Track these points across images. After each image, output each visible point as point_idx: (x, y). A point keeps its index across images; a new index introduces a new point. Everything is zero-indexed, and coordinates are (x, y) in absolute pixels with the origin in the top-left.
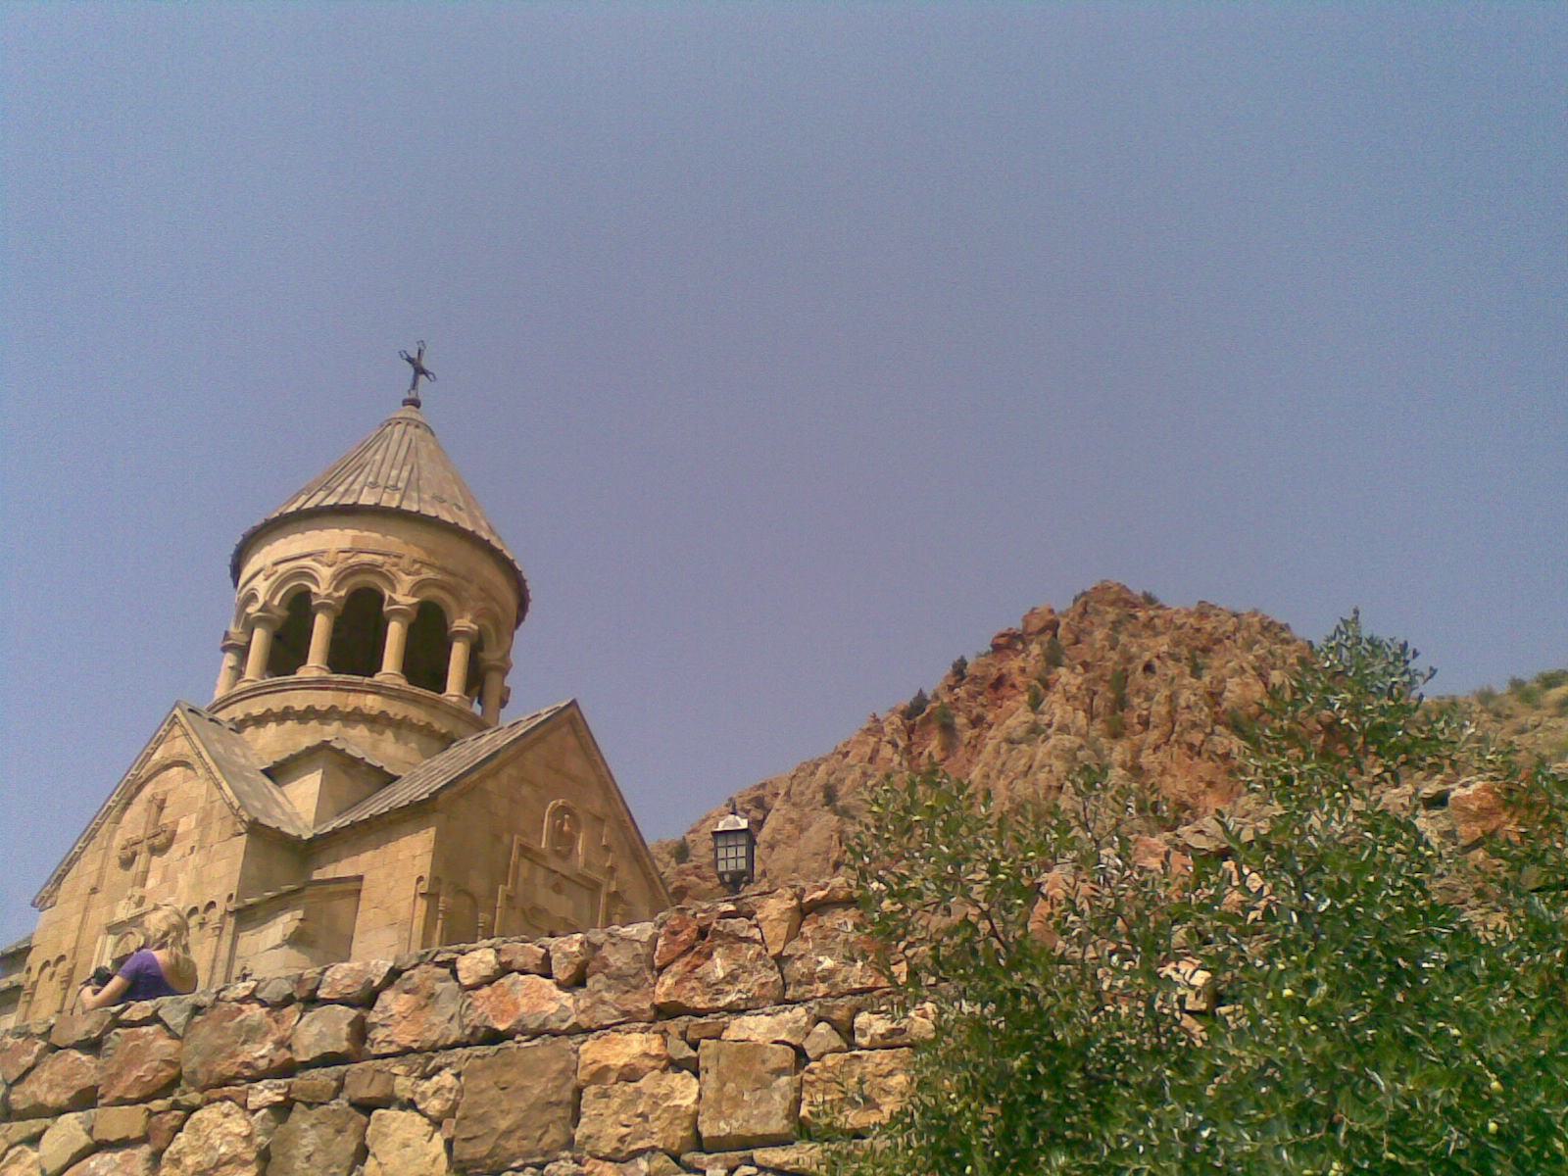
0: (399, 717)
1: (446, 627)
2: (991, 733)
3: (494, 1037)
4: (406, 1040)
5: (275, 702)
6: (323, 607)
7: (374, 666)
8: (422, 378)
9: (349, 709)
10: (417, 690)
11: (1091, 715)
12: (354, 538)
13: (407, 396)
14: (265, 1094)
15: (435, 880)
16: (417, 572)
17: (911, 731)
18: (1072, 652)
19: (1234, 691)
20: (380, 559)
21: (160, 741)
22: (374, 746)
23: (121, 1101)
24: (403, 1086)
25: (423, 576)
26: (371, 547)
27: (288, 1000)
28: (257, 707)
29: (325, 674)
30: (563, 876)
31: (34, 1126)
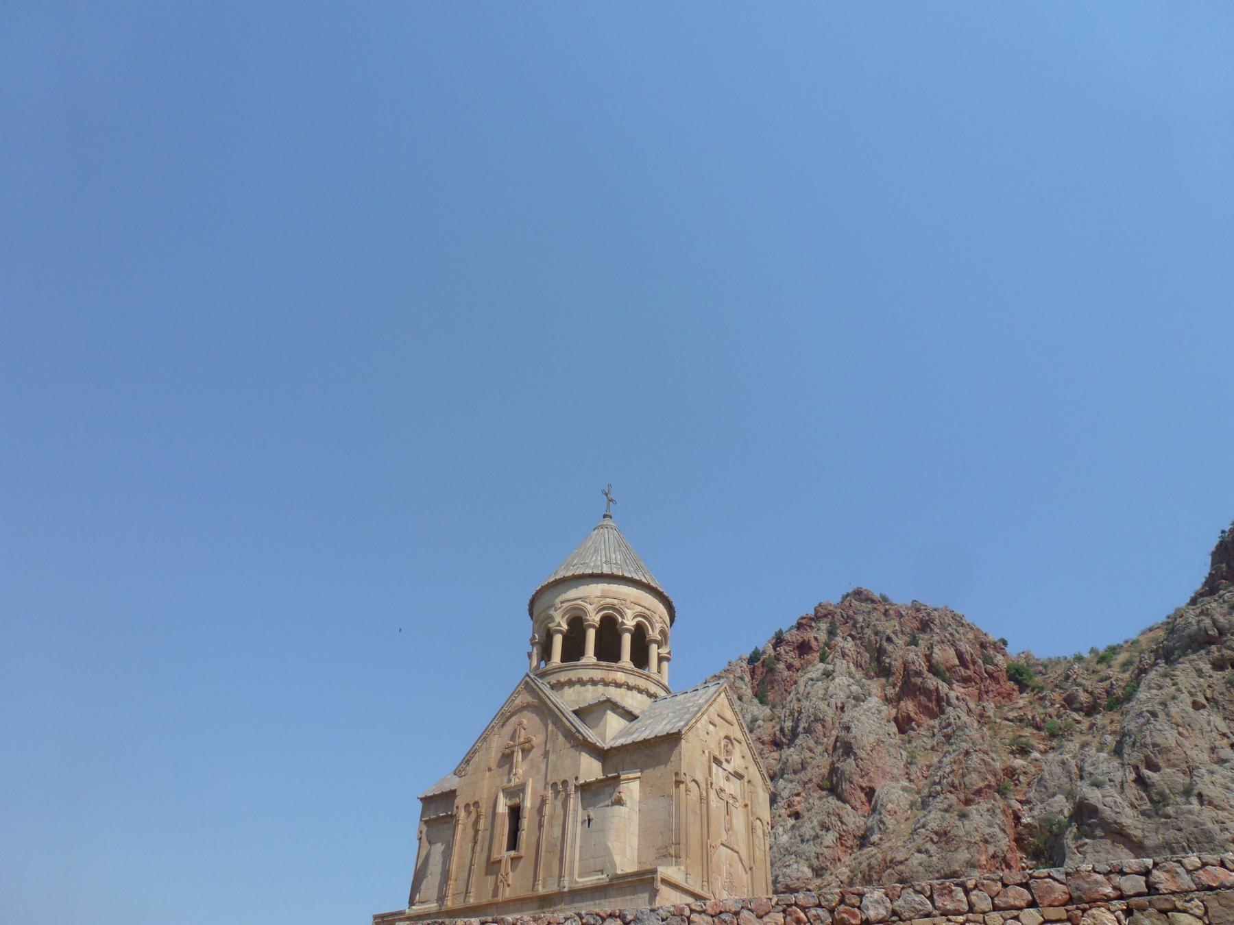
1: (644, 637)
2: (800, 673)
3: (1210, 888)
4: (1174, 888)
5: (573, 675)
7: (616, 657)
11: (858, 665)
12: (603, 591)
14: (1119, 905)
17: (753, 672)
18: (844, 628)
19: (938, 654)
20: (616, 601)
23: (1050, 906)
24: (1179, 904)
27: (1110, 872)
28: (563, 677)
31: (1015, 913)
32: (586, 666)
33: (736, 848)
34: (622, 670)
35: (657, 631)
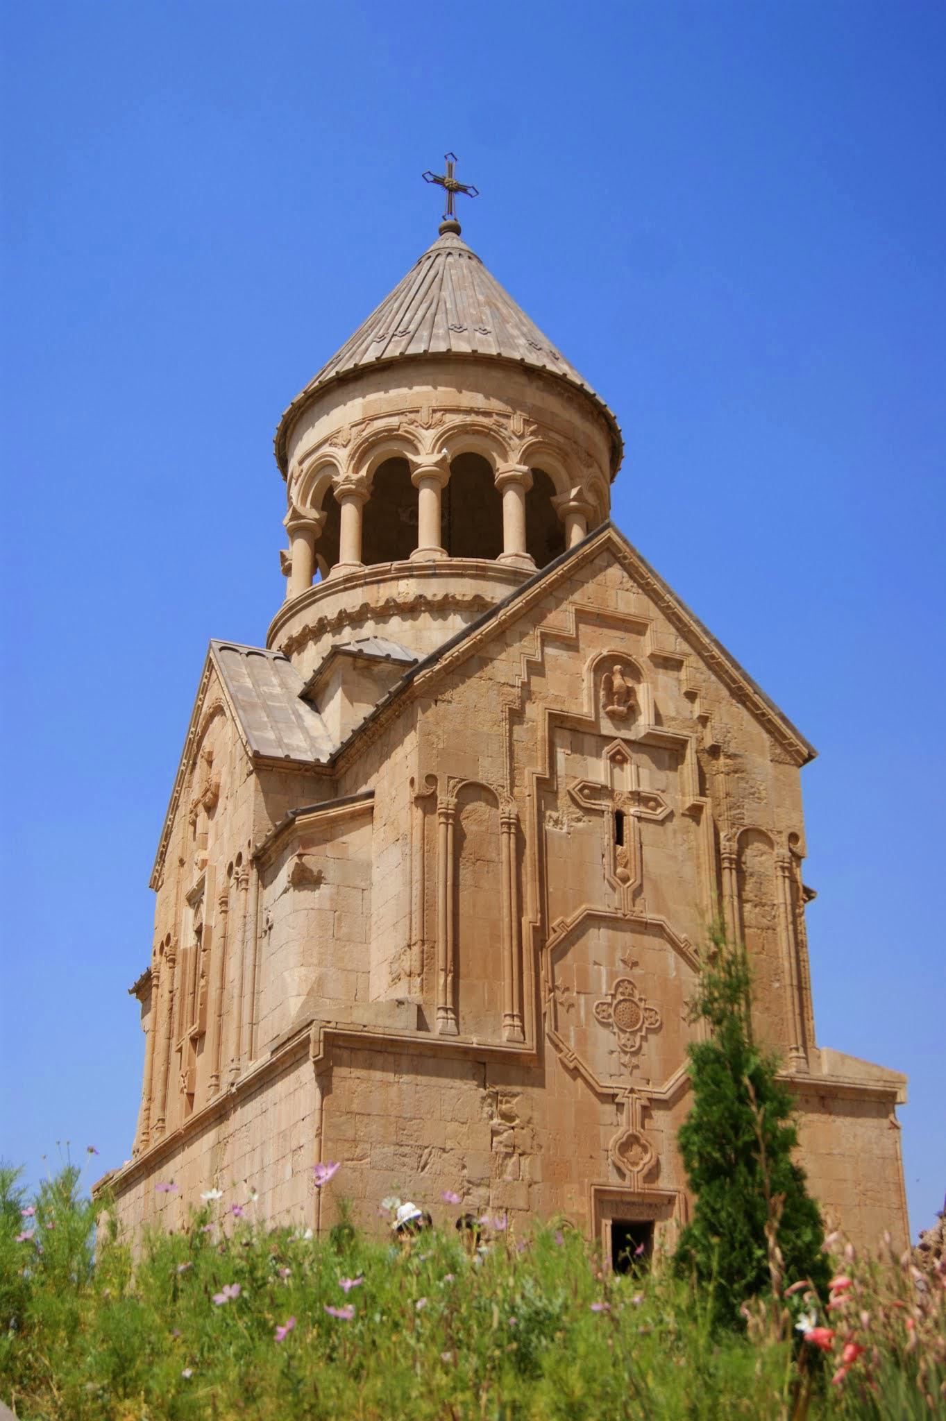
0: (439, 597)
6: (347, 494)
8: (459, 198)
9: (381, 603)
10: (456, 561)
12: (365, 408)
13: (444, 223)
15: (431, 779)
16: (441, 422)
20: (394, 421)
21: (204, 689)
22: (418, 638)
25: (446, 427)
26: (386, 409)
29: (354, 569)
30: (625, 741)
32: (332, 589)
33: (650, 916)
34: (409, 573)
35: (514, 457)
